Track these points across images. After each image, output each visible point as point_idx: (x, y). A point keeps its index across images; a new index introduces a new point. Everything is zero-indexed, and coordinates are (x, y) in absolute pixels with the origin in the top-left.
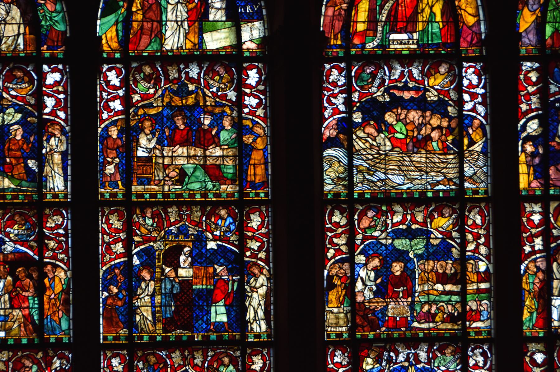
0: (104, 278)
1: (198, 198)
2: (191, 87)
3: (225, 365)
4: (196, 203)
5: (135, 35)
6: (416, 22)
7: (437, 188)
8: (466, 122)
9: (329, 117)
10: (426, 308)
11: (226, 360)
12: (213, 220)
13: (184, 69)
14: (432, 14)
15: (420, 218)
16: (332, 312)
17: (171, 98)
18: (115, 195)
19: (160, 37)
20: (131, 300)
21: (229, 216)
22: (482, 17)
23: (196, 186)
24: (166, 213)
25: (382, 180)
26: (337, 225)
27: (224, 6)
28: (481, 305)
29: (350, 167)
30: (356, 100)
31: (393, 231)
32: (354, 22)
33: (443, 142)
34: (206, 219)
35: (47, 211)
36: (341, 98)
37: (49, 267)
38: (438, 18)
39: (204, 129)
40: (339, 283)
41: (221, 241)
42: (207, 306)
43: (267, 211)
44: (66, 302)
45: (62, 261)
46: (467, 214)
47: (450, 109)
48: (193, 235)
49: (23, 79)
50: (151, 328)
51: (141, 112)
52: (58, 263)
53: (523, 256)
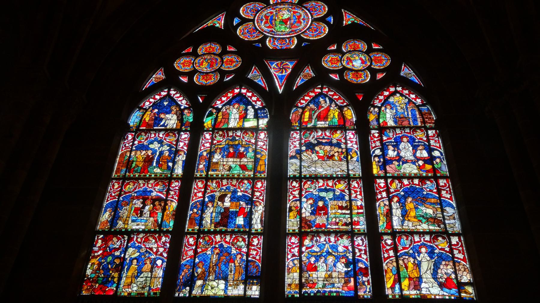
0: (192, 206)
1: (236, 176)
2: (237, 138)
3: (240, 242)
4: (235, 178)
5: (218, 123)
6: (327, 118)
7: (337, 173)
9: (292, 149)
10: (334, 220)
11: (241, 239)
12: (241, 184)
18: (202, 175)
19: (228, 123)
21: (248, 183)
23: (235, 172)
24: (222, 182)
25: (314, 170)
26: (294, 187)
29: (301, 165)
33: (340, 157)
34: (238, 184)
35: (173, 181)
36: (298, 142)
38: (337, 117)
41: (244, 192)
42: (235, 217)
43: (264, 181)
44: (173, 215)
45: (175, 199)
46: (351, 183)
50: (209, 226)
51: (216, 147)
52: (173, 200)
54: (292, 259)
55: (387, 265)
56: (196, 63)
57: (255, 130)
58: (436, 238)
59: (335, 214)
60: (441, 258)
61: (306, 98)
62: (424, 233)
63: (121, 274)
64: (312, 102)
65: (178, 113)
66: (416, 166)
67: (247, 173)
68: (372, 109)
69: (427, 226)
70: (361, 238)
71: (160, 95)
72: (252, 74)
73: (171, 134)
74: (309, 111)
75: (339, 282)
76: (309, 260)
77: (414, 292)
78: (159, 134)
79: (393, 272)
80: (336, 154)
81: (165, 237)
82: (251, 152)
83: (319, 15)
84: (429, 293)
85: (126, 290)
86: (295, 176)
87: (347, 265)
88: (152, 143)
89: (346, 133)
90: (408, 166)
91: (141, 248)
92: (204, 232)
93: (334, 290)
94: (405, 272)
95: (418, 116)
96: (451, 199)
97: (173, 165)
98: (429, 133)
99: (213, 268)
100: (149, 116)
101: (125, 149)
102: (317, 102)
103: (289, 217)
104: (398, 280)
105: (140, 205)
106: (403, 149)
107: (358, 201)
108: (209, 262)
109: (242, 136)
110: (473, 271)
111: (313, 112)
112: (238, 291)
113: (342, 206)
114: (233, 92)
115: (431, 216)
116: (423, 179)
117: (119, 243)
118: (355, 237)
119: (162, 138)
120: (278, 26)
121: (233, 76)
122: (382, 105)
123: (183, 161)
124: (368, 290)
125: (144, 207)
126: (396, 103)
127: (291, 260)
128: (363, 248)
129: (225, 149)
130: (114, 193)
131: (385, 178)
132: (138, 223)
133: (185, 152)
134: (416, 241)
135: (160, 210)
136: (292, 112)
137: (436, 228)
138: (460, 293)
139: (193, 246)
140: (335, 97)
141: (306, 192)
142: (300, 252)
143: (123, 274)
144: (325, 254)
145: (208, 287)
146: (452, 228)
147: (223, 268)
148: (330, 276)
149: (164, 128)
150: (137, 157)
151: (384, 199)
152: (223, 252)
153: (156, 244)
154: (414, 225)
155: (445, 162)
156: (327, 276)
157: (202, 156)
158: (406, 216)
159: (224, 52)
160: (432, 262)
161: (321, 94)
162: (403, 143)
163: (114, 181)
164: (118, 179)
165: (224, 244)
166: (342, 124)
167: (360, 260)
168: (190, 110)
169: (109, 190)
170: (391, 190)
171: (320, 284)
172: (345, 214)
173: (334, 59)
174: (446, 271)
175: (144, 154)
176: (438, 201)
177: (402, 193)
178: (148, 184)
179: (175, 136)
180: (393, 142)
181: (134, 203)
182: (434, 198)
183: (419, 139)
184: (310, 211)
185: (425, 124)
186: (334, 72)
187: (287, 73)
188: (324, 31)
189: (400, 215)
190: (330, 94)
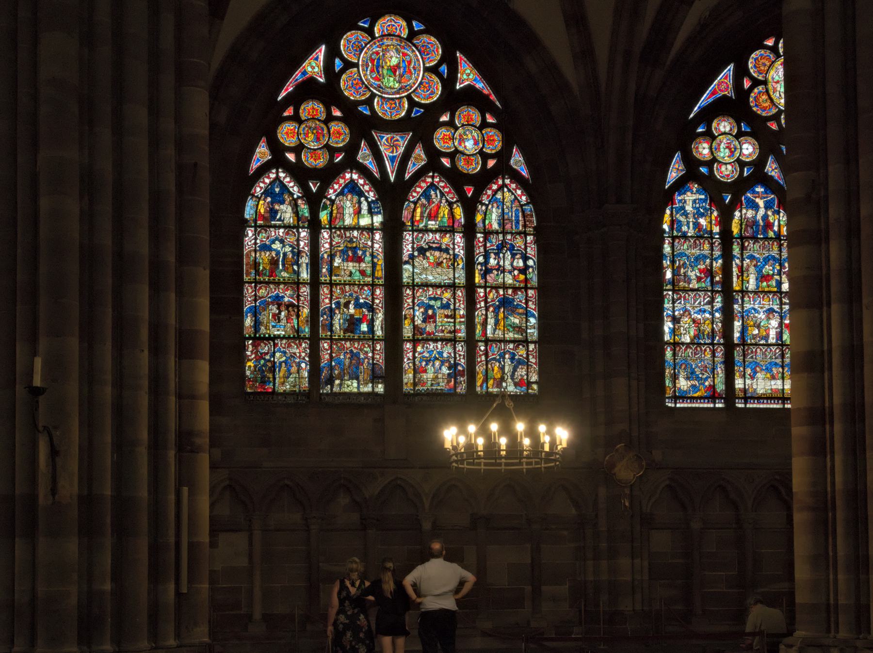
0: (322, 312)
1: (357, 283)
2: (355, 240)
4: (356, 284)
10: (441, 328)
11: (366, 346)
14: (444, 214)
15: (439, 293)
18: (325, 280)
19: (344, 221)
23: (356, 278)
24: (345, 288)
26: (408, 294)
29: (413, 272)
35: (301, 286)
38: (446, 216)
44: (307, 321)
45: (306, 305)
56: (301, 134)
57: (371, 229)
58: (518, 346)
60: (520, 362)
61: (418, 189)
62: (510, 341)
65: (292, 204)
67: (366, 278)
68: (480, 206)
71: (269, 177)
73: (291, 233)
75: (443, 382)
77: (496, 390)
78: (279, 232)
80: (445, 261)
83: (431, 61)
86: (408, 283)
87: (449, 368)
88: (273, 242)
89: (454, 235)
93: (439, 388)
96: (535, 310)
97: (298, 268)
101: (249, 248)
104: (486, 380)
110: (540, 374)
112: (368, 388)
113: (448, 315)
114: (344, 178)
116: (515, 289)
117: (266, 348)
119: (283, 237)
120: (386, 78)
121: (342, 155)
122: (490, 201)
125: (280, 313)
128: (462, 353)
130: (250, 298)
131: (485, 287)
135: (295, 316)
138: (528, 389)
140: (447, 190)
141: (418, 300)
142: (414, 357)
148: (437, 377)
149: (281, 222)
150: (262, 259)
152: (354, 356)
155: (536, 272)
159: (329, 118)
161: (432, 184)
163: (247, 285)
165: (353, 350)
171: (429, 383)
173: (446, 135)
175: (269, 255)
177: (497, 303)
178: (279, 289)
179: (295, 235)
180: (496, 250)
182: (522, 308)
185: (525, 228)
186: (446, 155)
188: (437, 89)
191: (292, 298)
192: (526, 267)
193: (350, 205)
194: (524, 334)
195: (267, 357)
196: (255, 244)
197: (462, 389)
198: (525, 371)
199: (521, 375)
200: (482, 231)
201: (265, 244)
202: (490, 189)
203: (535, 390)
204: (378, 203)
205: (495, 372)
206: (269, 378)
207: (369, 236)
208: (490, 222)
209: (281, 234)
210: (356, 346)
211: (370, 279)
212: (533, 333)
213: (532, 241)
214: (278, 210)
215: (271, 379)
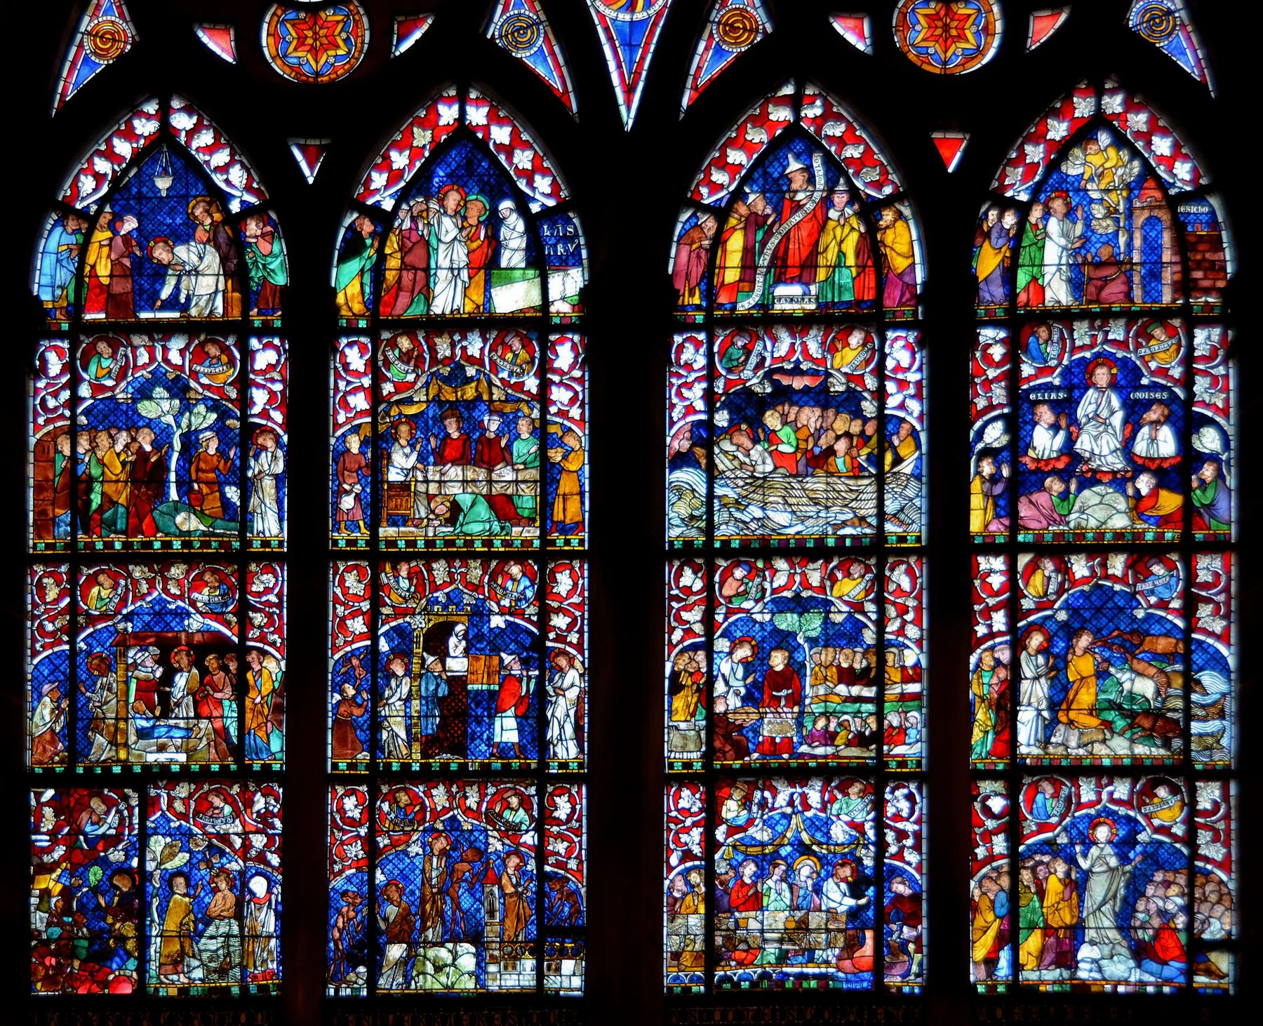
1: (478, 546)
2: (471, 371)
3: (512, 809)
4: (475, 555)
7: (841, 532)
8: (890, 427)
9: (679, 419)
10: (821, 723)
11: (514, 801)
12: (500, 581)
13: (460, 341)
14: (842, 254)
15: (815, 578)
16: (677, 728)
17: (440, 388)
18: (351, 543)
19: (428, 295)
20: (375, 706)
21: (524, 575)
22: (918, 258)
23: (475, 528)
24: (430, 570)
25: (758, 520)
26: (688, 590)
27: (524, 245)
28: (906, 719)
29: (710, 495)
30: (720, 391)
31: (773, 601)
32: (720, 268)
33: (853, 458)
34: (489, 580)
35: (253, 567)
36: (699, 388)
37: (254, 654)
38: (851, 261)
39: (489, 440)
40: (689, 683)
41: (511, 614)
43: (581, 568)
44: (277, 709)
45: (273, 644)
46: (887, 573)
47: (865, 405)
48: (469, 605)
49: (219, 359)
50: (405, 752)
52: (267, 648)
53: (973, 642)
54: (682, 867)
55: (980, 886)
58: (1149, 792)
59: (826, 701)
61: (736, 156)
63: (145, 925)
64: (755, 181)
66: (1127, 497)
67: (516, 530)
69: (1126, 744)
70: (905, 791)
71: (130, 135)
72: (503, 12)
73: (213, 350)
74: (745, 228)
75: (829, 945)
76: (737, 873)
77: (1052, 974)
78: (166, 350)
79: (997, 910)
80: (841, 446)
81: (263, 795)
82: (525, 435)
84: (1097, 976)
85: (170, 977)
86: (688, 544)
87: (856, 890)
88: (144, 393)
89: (883, 340)
90: (1097, 499)
91: (191, 835)
92: (389, 776)
93: (811, 970)
94: (1034, 908)
95: (1167, 256)
96: (1224, 637)
97: (245, 498)
98: (1197, 341)
99: (434, 902)
100: (105, 250)
101: (48, 422)
102: (776, 181)
103: (670, 712)
104: (1010, 937)
105: (153, 672)
106: (1089, 420)
107: (908, 647)
108: (418, 881)
109: (487, 360)
111: (760, 235)
112: (521, 976)
114: (431, 122)
115: (1146, 706)
117: (112, 818)
118: (888, 789)
119: (181, 368)
121: (425, 27)
122: (1036, 192)
123: (277, 477)
124: (915, 968)
125: (168, 679)
126: (1089, 187)
127: (679, 874)
128: (910, 827)
129: (427, 424)
130: (52, 620)
131: (1010, 550)
132: (160, 741)
133: (277, 438)
134: (1084, 799)
135: (228, 690)
136: (677, 232)
137: (1155, 751)
138: (1189, 973)
139: (360, 824)
140: (853, 152)
142: (710, 844)
143: (150, 926)
144: (789, 849)
145: (424, 964)
146: (1208, 753)
147: (466, 902)
148: (803, 926)
149: (176, 315)
150: (101, 462)
151: (998, 640)
153: (237, 821)
154: (1085, 739)
155: (1231, 481)
156: (792, 925)
157: (343, 454)
158: (1064, 706)
160: (1124, 874)
162: (1091, 391)
163: (39, 569)
164: (50, 560)
166: (869, 295)
167: (897, 868)
168: (267, 221)
169: (29, 607)
170: (1023, 601)
171: (771, 951)
172: (860, 699)
174: (1161, 903)
175: (127, 446)
176: (1181, 645)
177: (1062, 616)
178: (165, 580)
180: (1058, 389)
181: (130, 661)
182: (1167, 635)
183: (1153, 373)
184: (743, 691)
187: (651, 12)
189: (1044, 705)
190: (830, 133)
191: (219, 617)
192: (1190, 458)
193: (454, 232)
194: (1177, 743)
195: (116, 855)
196: (75, 401)
197: (907, 973)
198: (1182, 895)
199: (1162, 913)
200: (1000, 313)
201: (113, 398)
202: (1038, 138)
203: (1223, 976)
204: (569, 221)
205: (1050, 899)
206: (122, 939)
207: (531, 353)
208: (1035, 279)
209: (175, 358)
210: (472, 802)
211: (532, 533)
212: (1217, 736)
213: (1214, 350)
214: (169, 265)
215: (130, 945)
